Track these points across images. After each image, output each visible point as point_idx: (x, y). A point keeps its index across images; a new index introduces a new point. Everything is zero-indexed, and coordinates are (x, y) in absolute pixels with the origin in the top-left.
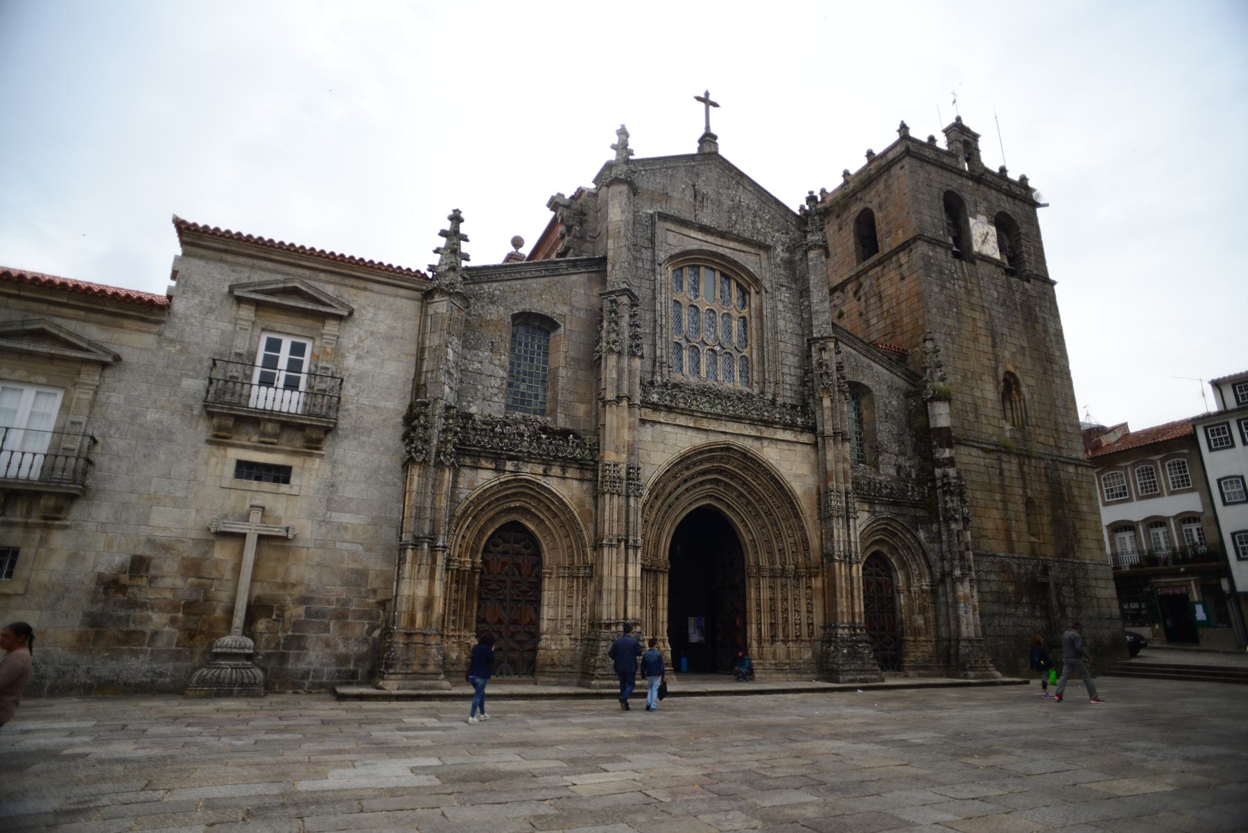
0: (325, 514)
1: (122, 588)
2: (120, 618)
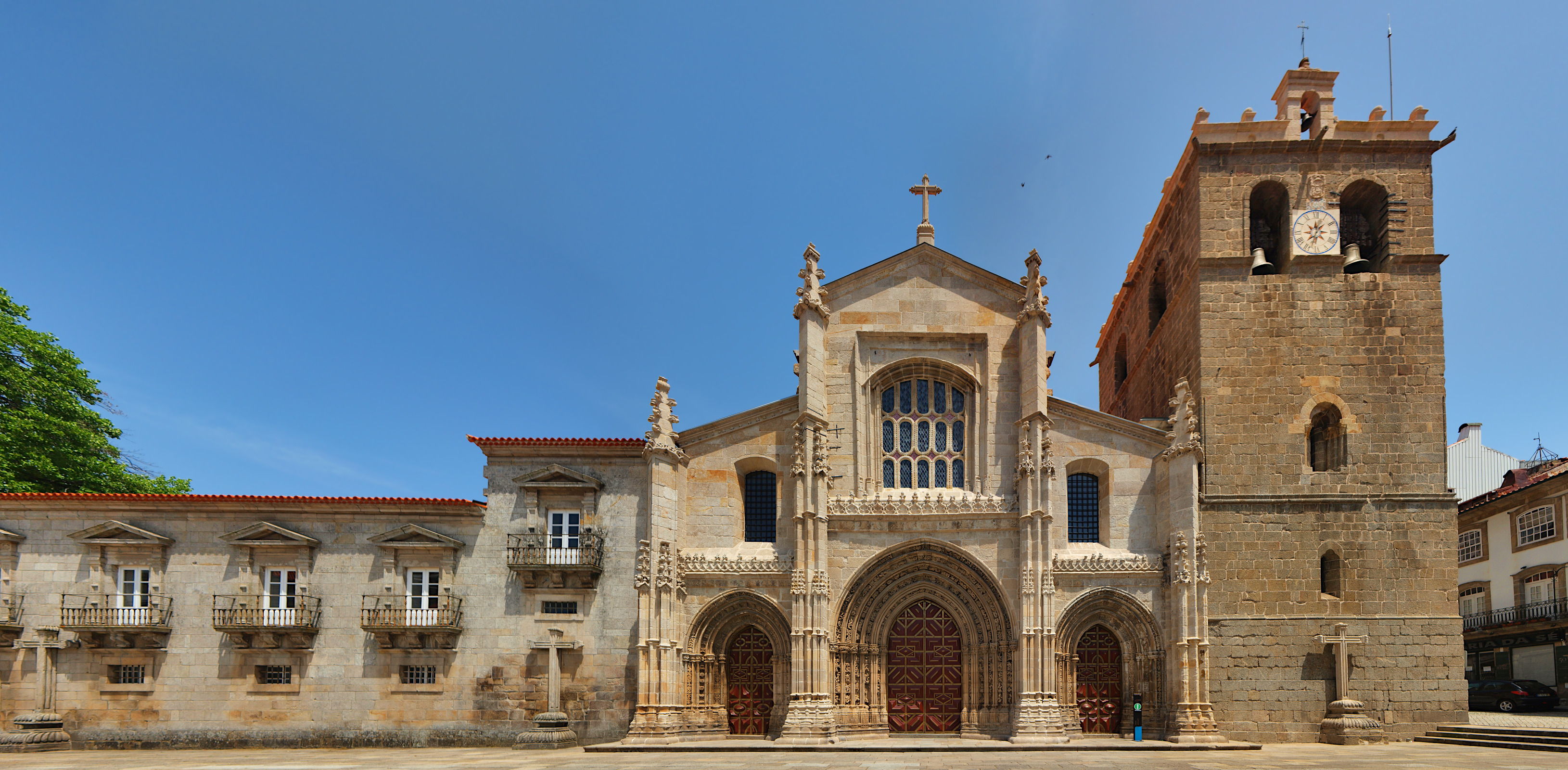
0: (602, 632)
1: (490, 686)
2: (492, 704)
